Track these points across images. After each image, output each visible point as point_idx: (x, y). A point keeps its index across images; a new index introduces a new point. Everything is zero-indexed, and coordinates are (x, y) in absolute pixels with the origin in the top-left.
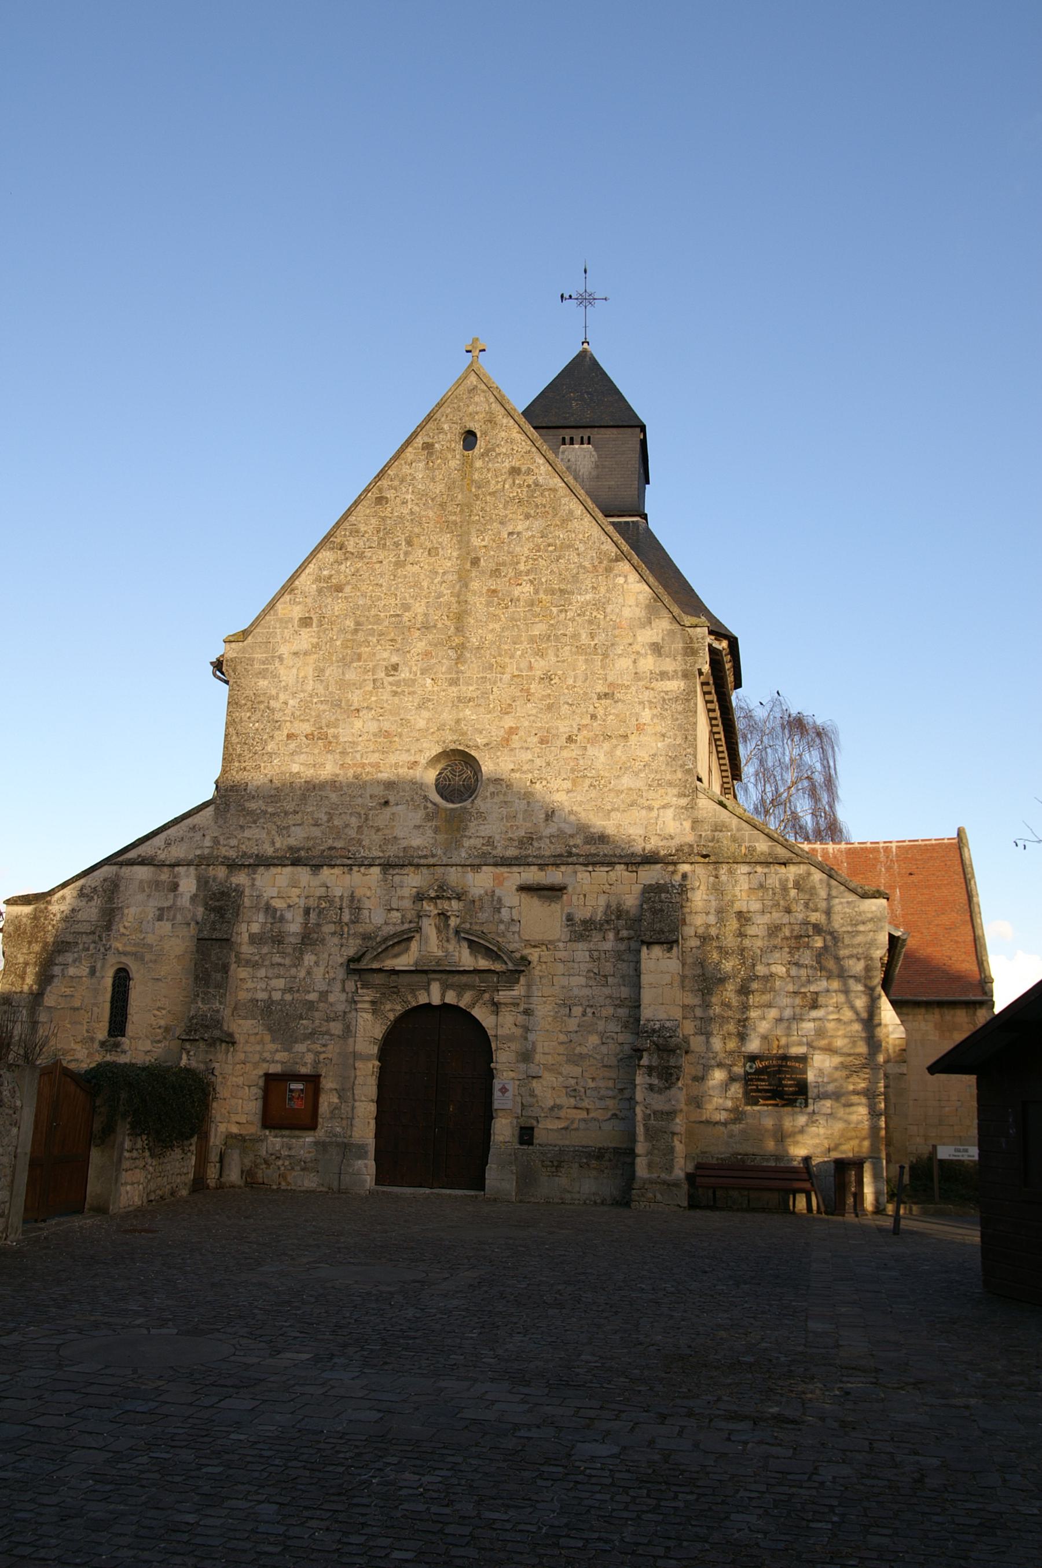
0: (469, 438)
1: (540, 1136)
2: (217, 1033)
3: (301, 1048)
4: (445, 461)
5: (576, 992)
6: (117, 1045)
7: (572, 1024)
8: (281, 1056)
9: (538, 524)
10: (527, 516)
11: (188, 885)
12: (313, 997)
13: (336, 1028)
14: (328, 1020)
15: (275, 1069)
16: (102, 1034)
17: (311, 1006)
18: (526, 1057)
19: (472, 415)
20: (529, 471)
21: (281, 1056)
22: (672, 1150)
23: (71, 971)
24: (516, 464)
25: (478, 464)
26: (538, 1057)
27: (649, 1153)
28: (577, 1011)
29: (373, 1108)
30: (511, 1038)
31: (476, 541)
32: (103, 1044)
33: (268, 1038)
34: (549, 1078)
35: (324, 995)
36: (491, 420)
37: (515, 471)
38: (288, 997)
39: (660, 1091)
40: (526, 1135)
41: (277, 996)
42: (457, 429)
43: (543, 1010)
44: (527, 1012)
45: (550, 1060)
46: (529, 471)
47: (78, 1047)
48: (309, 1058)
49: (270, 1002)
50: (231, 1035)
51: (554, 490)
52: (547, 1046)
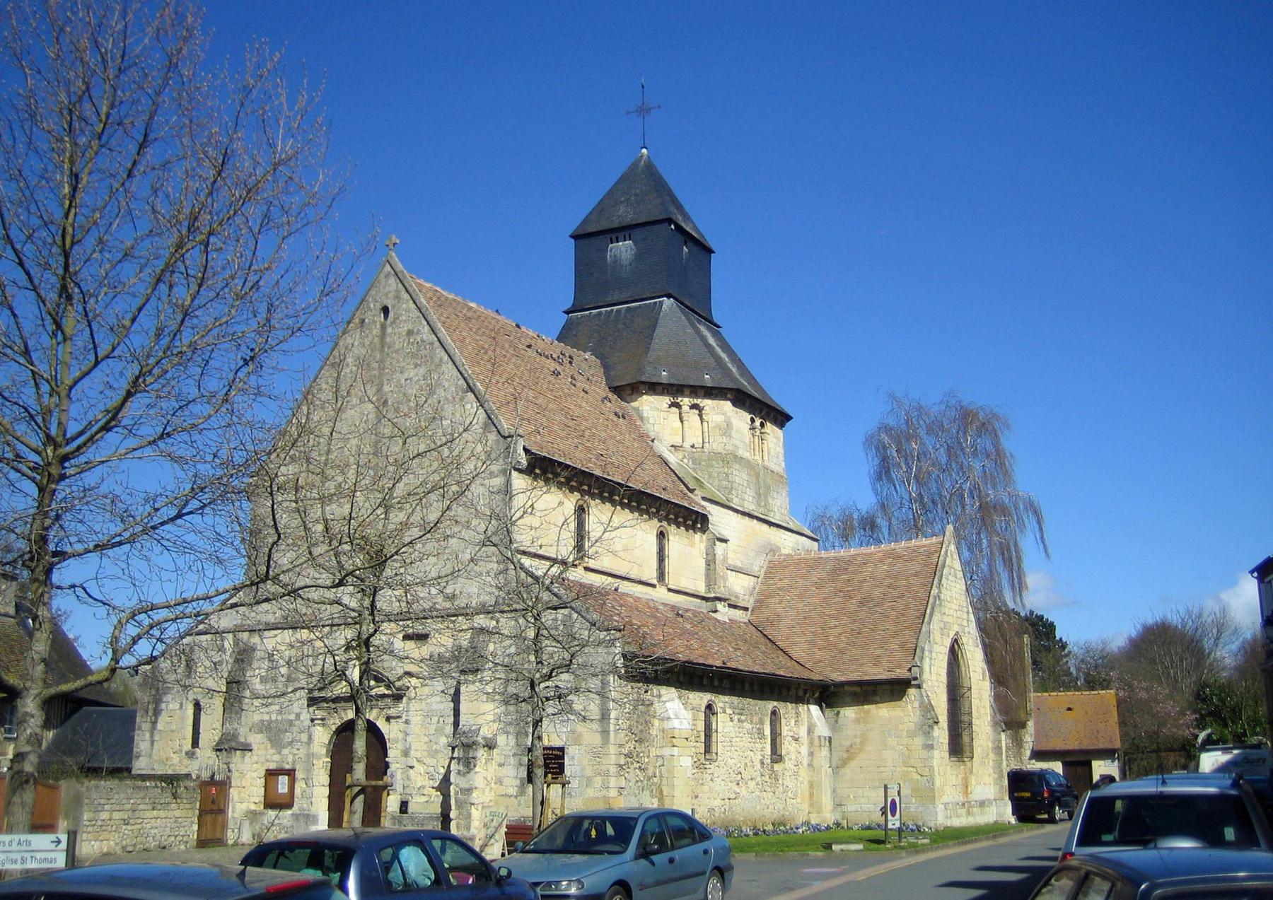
0: (385, 310)
1: (411, 808)
2: (233, 744)
3: (285, 751)
4: (370, 330)
5: (435, 707)
6: (193, 754)
7: (432, 729)
8: (277, 757)
9: (422, 370)
10: (416, 365)
11: (229, 641)
12: (292, 717)
13: (304, 737)
14: (301, 732)
15: (273, 766)
16: (188, 745)
17: (291, 723)
18: (406, 753)
19: (386, 295)
20: (419, 332)
21: (277, 757)
22: (469, 816)
23: (171, 706)
24: (410, 327)
25: (389, 330)
26: (412, 753)
27: (458, 817)
28: (435, 719)
29: (326, 791)
30: (396, 741)
31: (386, 388)
32: (187, 753)
33: (269, 746)
34: (420, 768)
35: (298, 715)
36: (397, 297)
37: (410, 333)
38: (279, 718)
39: (464, 775)
40: (404, 806)
41: (274, 717)
42: (379, 306)
43: (416, 719)
44: (407, 722)
45: (419, 755)
46: (419, 332)
47: (174, 756)
48: (290, 758)
49: (270, 722)
50: (250, 745)
51: (432, 344)
52: (418, 747)
